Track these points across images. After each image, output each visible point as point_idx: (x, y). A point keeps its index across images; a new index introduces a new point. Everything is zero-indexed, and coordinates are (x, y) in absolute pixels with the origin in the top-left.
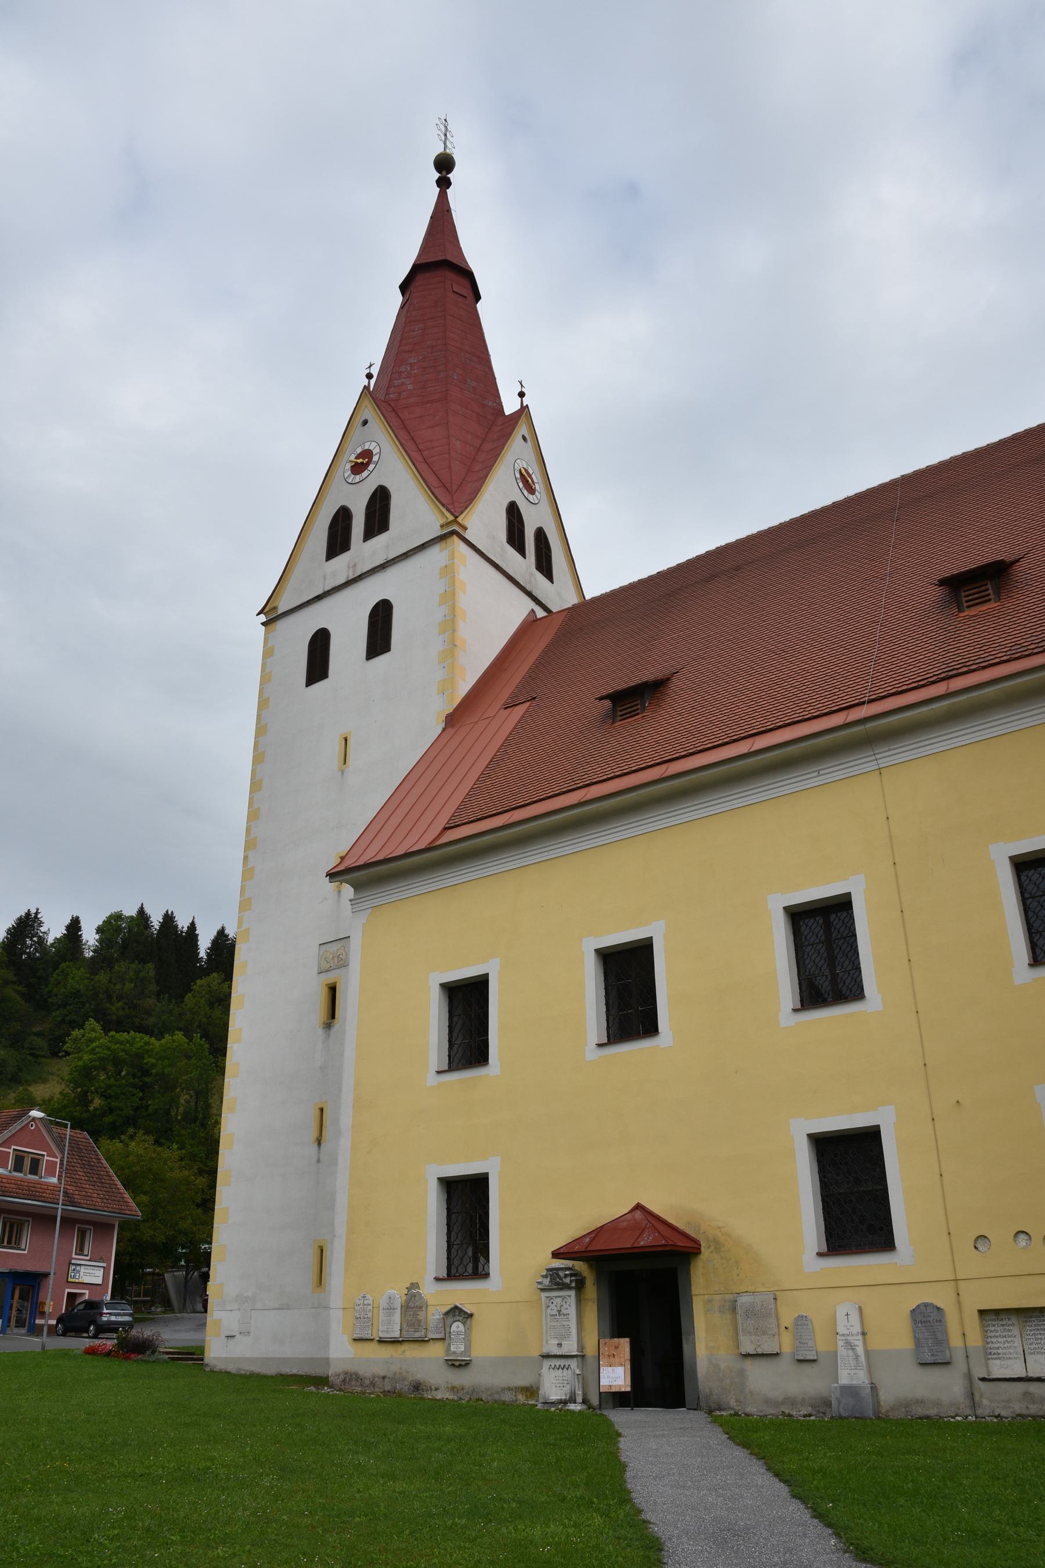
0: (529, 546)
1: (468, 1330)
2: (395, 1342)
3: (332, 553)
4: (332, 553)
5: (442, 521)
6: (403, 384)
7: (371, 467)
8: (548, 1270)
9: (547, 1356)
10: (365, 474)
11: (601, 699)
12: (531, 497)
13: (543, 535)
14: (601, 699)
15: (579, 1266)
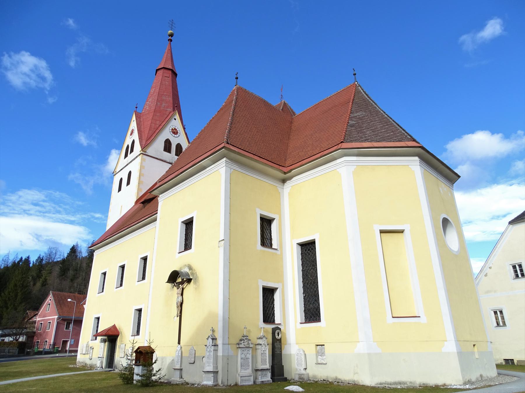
0: (173, 149)
1: (93, 351)
2: (84, 354)
3: (125, 158)
4: (125, 158)
5: (140, 151)
6: (147, 107)
7: (133, 134)
8: (101, 338)
9: (99, 357)
10: (132, 135)
11: (140, 203)
12: (176, 136)
13: (179, 145)
14: (140, 203)
15: (106, 337)
